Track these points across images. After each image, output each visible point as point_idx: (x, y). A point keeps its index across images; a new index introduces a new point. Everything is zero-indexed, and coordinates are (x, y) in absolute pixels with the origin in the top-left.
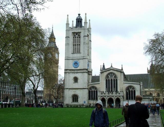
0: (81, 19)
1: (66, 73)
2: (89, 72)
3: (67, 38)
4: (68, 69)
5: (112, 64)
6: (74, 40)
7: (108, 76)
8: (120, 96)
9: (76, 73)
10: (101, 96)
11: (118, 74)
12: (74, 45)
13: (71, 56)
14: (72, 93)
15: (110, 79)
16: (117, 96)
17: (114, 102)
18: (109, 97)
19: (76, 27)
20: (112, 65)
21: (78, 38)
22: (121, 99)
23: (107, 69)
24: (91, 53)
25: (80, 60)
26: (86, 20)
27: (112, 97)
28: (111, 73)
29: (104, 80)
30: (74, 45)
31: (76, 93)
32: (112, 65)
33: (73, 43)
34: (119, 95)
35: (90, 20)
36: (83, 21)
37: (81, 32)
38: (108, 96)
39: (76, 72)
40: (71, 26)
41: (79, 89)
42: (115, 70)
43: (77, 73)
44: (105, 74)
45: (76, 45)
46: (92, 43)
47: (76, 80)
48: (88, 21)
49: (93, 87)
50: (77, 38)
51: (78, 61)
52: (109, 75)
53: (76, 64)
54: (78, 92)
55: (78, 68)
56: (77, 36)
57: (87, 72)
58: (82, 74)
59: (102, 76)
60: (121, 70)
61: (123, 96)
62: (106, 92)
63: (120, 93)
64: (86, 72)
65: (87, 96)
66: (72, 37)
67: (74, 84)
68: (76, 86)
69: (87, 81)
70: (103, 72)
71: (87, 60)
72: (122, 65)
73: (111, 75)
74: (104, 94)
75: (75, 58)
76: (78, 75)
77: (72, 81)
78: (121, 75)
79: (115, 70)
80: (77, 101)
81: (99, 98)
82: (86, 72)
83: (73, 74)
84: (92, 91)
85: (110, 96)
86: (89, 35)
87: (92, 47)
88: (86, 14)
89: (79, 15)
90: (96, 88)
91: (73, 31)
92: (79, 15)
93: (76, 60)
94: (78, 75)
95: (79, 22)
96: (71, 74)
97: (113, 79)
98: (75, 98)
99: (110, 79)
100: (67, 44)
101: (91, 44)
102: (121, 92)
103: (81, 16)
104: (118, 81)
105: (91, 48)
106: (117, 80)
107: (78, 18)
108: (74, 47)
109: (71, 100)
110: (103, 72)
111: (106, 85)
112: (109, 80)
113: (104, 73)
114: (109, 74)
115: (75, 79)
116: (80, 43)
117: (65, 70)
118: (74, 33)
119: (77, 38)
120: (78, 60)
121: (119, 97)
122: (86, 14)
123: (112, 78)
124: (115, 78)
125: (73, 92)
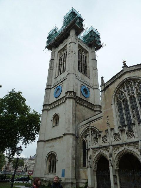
4: (47, 103)
7: (122, 92)
9: (56, 106)
10: (95, 149)
15: (128, 98)
18: (121, 149)
25: (64, 81)
27: (131, 148)
28: (127, 81)
29: (113, 106)
32: (125, 65)
38: (118, 146)
39: (57, 104)
41: (59, 139)
43: (58, 106)
51: (61, 85)
52: (124, 90)
55: (60, 97)
57: (72, 95)
62: (107, 131)
65: (70, 156)
69: (71, 116)
70: (108, 87)
73: (127, 87)
74: (101, 140)
75: (59, 83)
82: (69, 98)
83: (54, 109)
85: (121, 145)
94: (59, 110)
96: (50, 111)
98: (53, 162)
99: (128, 98)
110: (108, 87)
111: (118, 118)
112: (125, 101)
113: (110, 87)
114: (121, 86)
119: (63, 55)
120: (61, 83)
123: (133, 93)
125: (51, 147)
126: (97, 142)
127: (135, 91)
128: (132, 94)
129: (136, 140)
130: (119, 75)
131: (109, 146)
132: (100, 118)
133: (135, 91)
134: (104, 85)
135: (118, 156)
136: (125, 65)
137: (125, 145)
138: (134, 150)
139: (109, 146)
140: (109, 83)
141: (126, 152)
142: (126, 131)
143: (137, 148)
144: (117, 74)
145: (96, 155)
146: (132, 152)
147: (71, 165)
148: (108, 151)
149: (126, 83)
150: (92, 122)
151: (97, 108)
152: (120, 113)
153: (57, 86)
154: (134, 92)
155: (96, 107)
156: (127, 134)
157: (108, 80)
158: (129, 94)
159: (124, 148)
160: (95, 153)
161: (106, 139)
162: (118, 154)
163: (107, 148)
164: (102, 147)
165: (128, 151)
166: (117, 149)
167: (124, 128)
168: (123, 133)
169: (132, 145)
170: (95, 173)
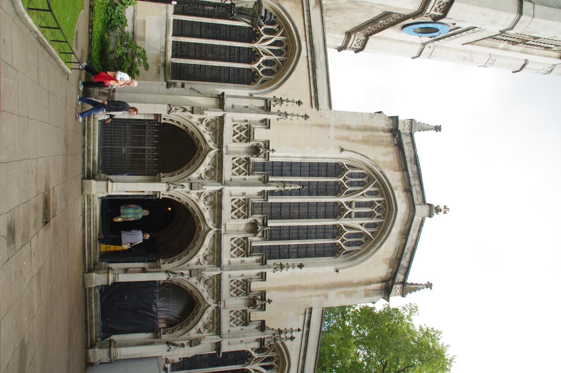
7: (363, 184)
15: (342, 200)
16: (218, 297)
18: (207, 215)
22: (193, 343)
27: (208, 242)
34: (225, 317)
42: (405, 234)
52: (370, 194)
59: (372, 129)
60: (404, 283)
63: (246, 321)
70: (399, 146)
73: (371, 204)
78: (370, 283)
79: (405, 234)
81: (201, 101)
84: (253, 36)
85: (218, 220)
97: (342, 222)
99: (342, 200)
102: (260, 335)
110: (399, 146)
112: (337, 190)
121: (206, 317)
123: (349, 216)
124: (349, 236)
126: (240, 139)
128: (347, 213)
129: (226, 259)
130: (415, 189)
131: (220, 181)
132: (313, 101)
134: (411, 135)
135: (191, 204)
136: (433, 210)
137: (218, 231)
138: (202, 251)
139: (220, 181)
140: (407, 154)
141: (200, 227)
142: (251, 238)
143: (205, 258)
144: (421, 184)
145: (202, 128)
146: (198, 243)
148: (207, 173)
149: (384, 204)
150: (310, 66)
151: (355, 42)
152: (311, 165)
154: (350, 217)
155: (364, 38)
156: (244, 238)
157: (419, 153)
158: (350, 204)
159: (211, 227)
160: (208, 125)
161: (243, 171)
162: (197, 206)
163: (217, 172)
164: (220, 152)
165: (202, 234)
166: (211, 203)
167: (260, 234)
168: (249, 227)
169: (214, 245)
170: (152, 118)
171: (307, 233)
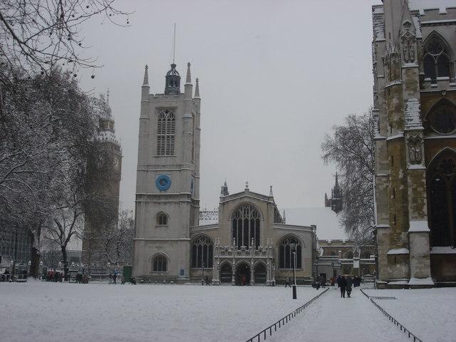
0: (178, 78)
1: (140, 202)
2: (193, 201)
3: (145, 120)
5: (247, 183)
6: (159, 124)
8: (265, 260)
10: (221, 259)
11: (262, 208)
12: (159, 137)
13: (153, 161)
14: (153, 251)
15: (243, 219)
17: (252, 271)
19: (167, 92)
20: (247, 186)
21: (169, 120)
23: (236, 195)
24: (199, 158)
26: (189, 79)
28: (246, 205)
30: (159, 137)
31: (162, 252)
32: (247, 186)
33: (159, 132)
35: (197, 81)
36: (183, 82)
37: (177, 107)
40: (153, 91)
43: (165, 203)
44: (232, 206)
45: (164, 137)
46: (202, 133)
47: (162, 219)
48: (193, 82)
49: (203, 238)
50: (166, 122)
53: (163, 182)
54: (167, 251)
56: (167, 116)
58: (177, 206)
61: (273, 260)
63: (265, 252)
64: (188, 202)
65: (188, 259)
66: (157, 119)
67: (158, 230)
68: (162, 233)
71: (190, 173)
72: (271, 187)
73: (245, 210)
76: (168, 209)
77: (153, 222)
78: (268, 210)
80: (165, 269)
84: (200, 247)
86: (195, 114)
87: (201, 143)
88: (189, 65)
89: (173, 66)
90: (209, 241)
91: (160, 105)
92: (173, 66)
93: (164, 173)
95: (171, 83)
99: (243, 219)
100: (143, 136)
101: (199, 135)
103: (177, 69)
104: (262, 224)
105: (199, 146)
106: (258, 221)
107: (171, 74)
108: (159, 142)
109: (150, 266)
112: (240, 221)
114: (240, 207)
115: (161, 218)
116: (173, 132)
117: (138, 196)
118: (159, 109)
119: (166, 122)
122: (189, 65)
125: (156, 247)
127: (250, 215)
133: (250, 215)
147: (188, 266)
153: (162, 173)
171: (252, 228)
